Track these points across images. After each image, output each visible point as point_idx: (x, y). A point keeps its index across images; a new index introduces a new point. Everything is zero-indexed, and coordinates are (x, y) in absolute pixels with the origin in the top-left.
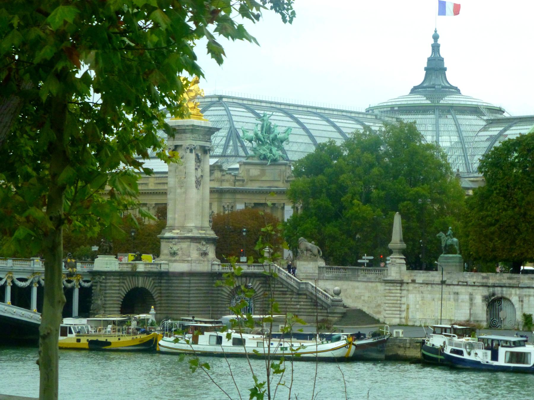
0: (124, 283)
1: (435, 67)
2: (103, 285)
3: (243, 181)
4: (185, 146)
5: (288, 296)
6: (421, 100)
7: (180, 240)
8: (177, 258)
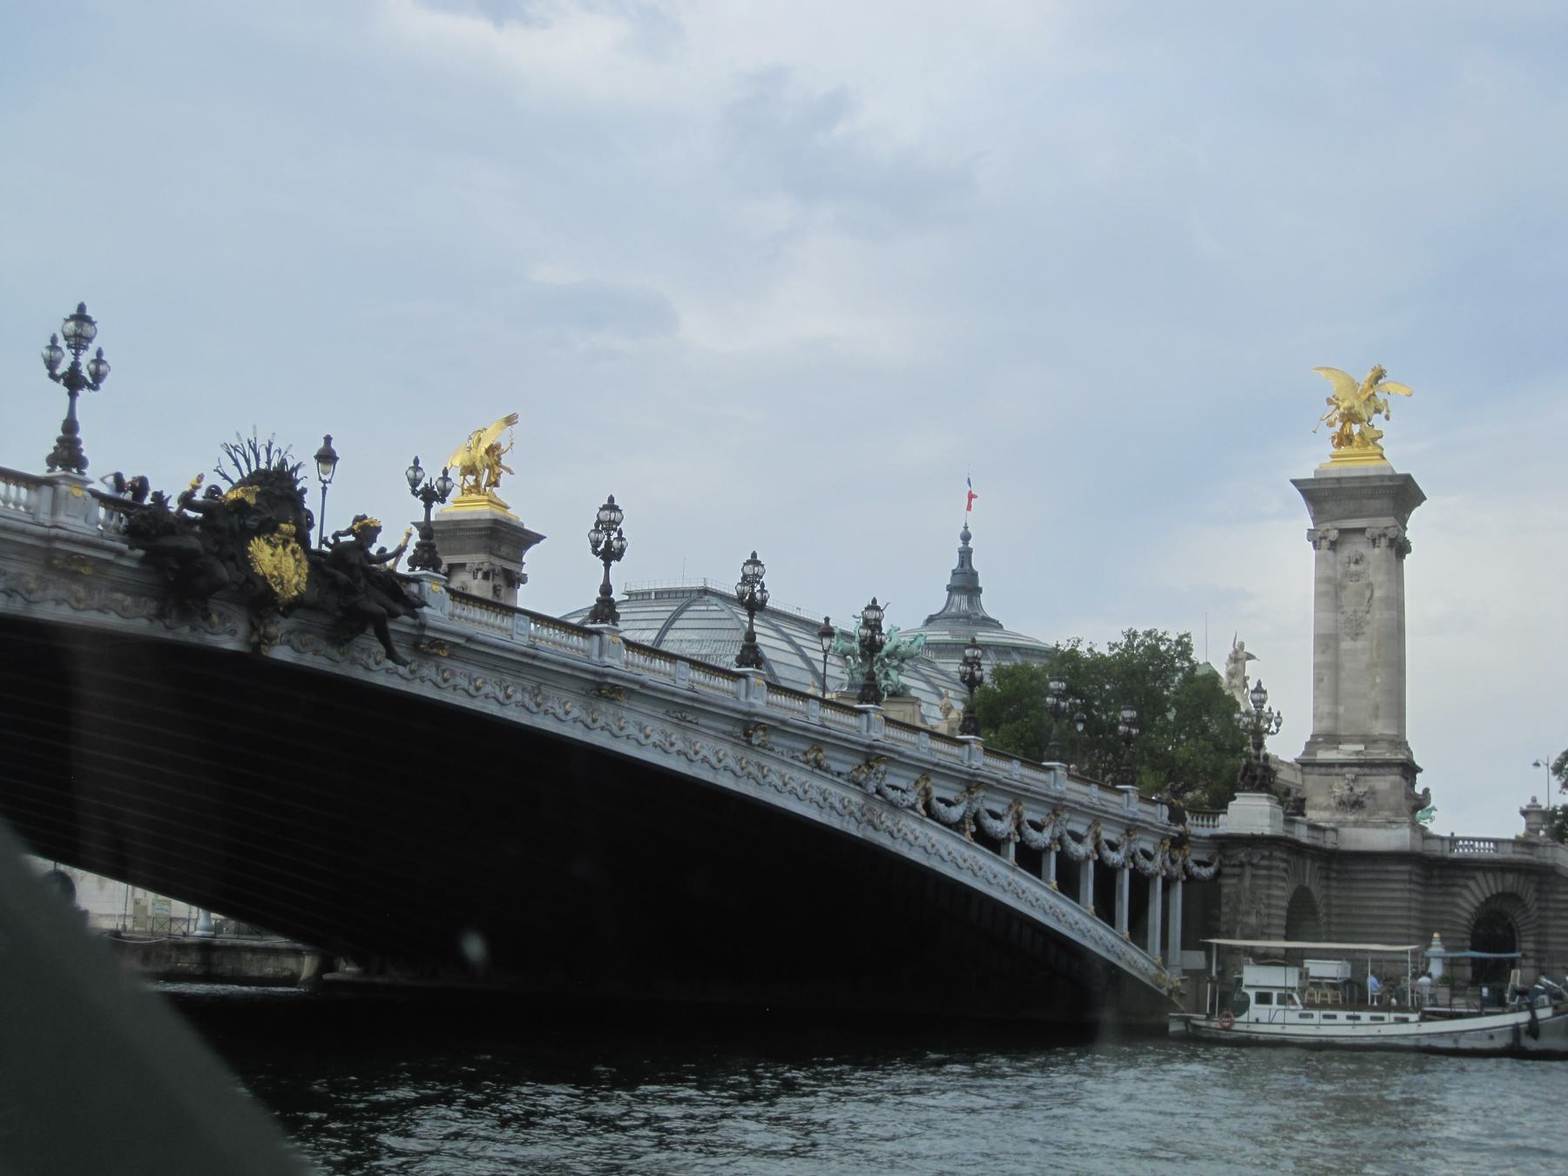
0: (1286, 870)
1: (966, 583)
6: (941, 635)
7: (1366, 770)
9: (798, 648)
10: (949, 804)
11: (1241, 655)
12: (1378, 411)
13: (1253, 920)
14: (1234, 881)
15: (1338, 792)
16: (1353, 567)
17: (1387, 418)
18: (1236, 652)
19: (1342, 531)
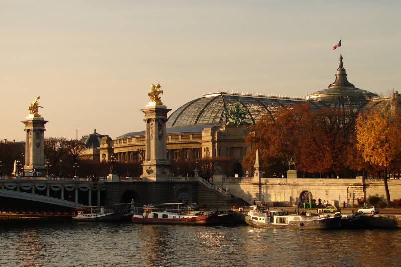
3: (224, 136)
13: (109, 198)
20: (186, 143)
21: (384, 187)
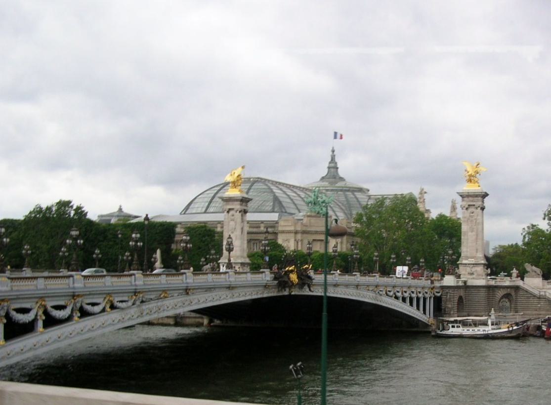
1: (333, 166)
2: (452, 295)
3: (307, 226)
4: (477, 206)
5: (531, 299)
8: (474, 276)
9: (288, 195)
10: (390, 291)
11: (423, 192)
12: (478, 173)
13: (450, 306)
14: (445, 297)
15: (468, 271)
16: (472, 214)
17: (480, 175)
18: (421, 191)
19: (469, 205)
20: (255, 233)
21: (328, 279)
